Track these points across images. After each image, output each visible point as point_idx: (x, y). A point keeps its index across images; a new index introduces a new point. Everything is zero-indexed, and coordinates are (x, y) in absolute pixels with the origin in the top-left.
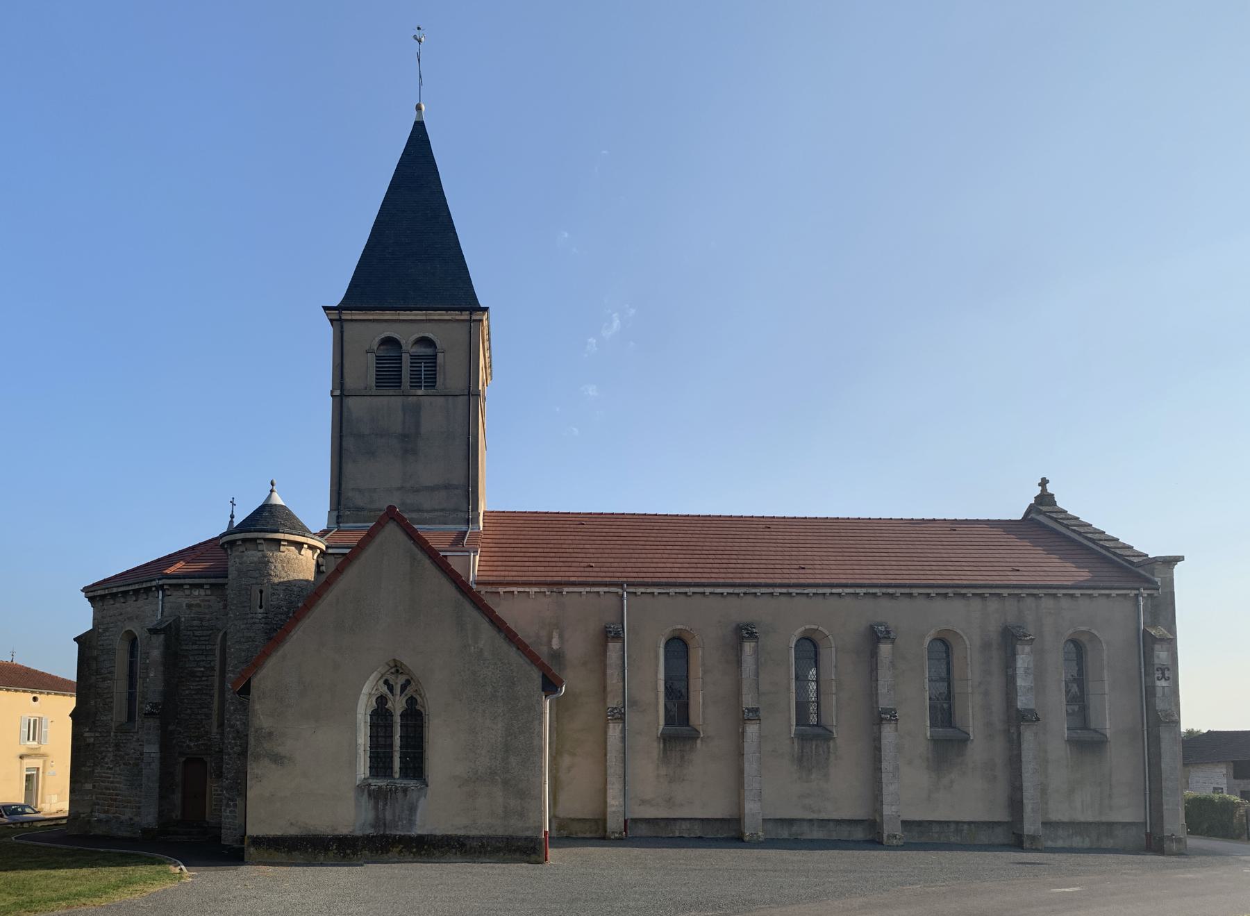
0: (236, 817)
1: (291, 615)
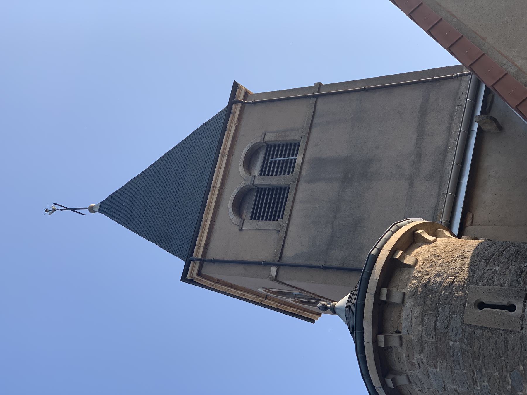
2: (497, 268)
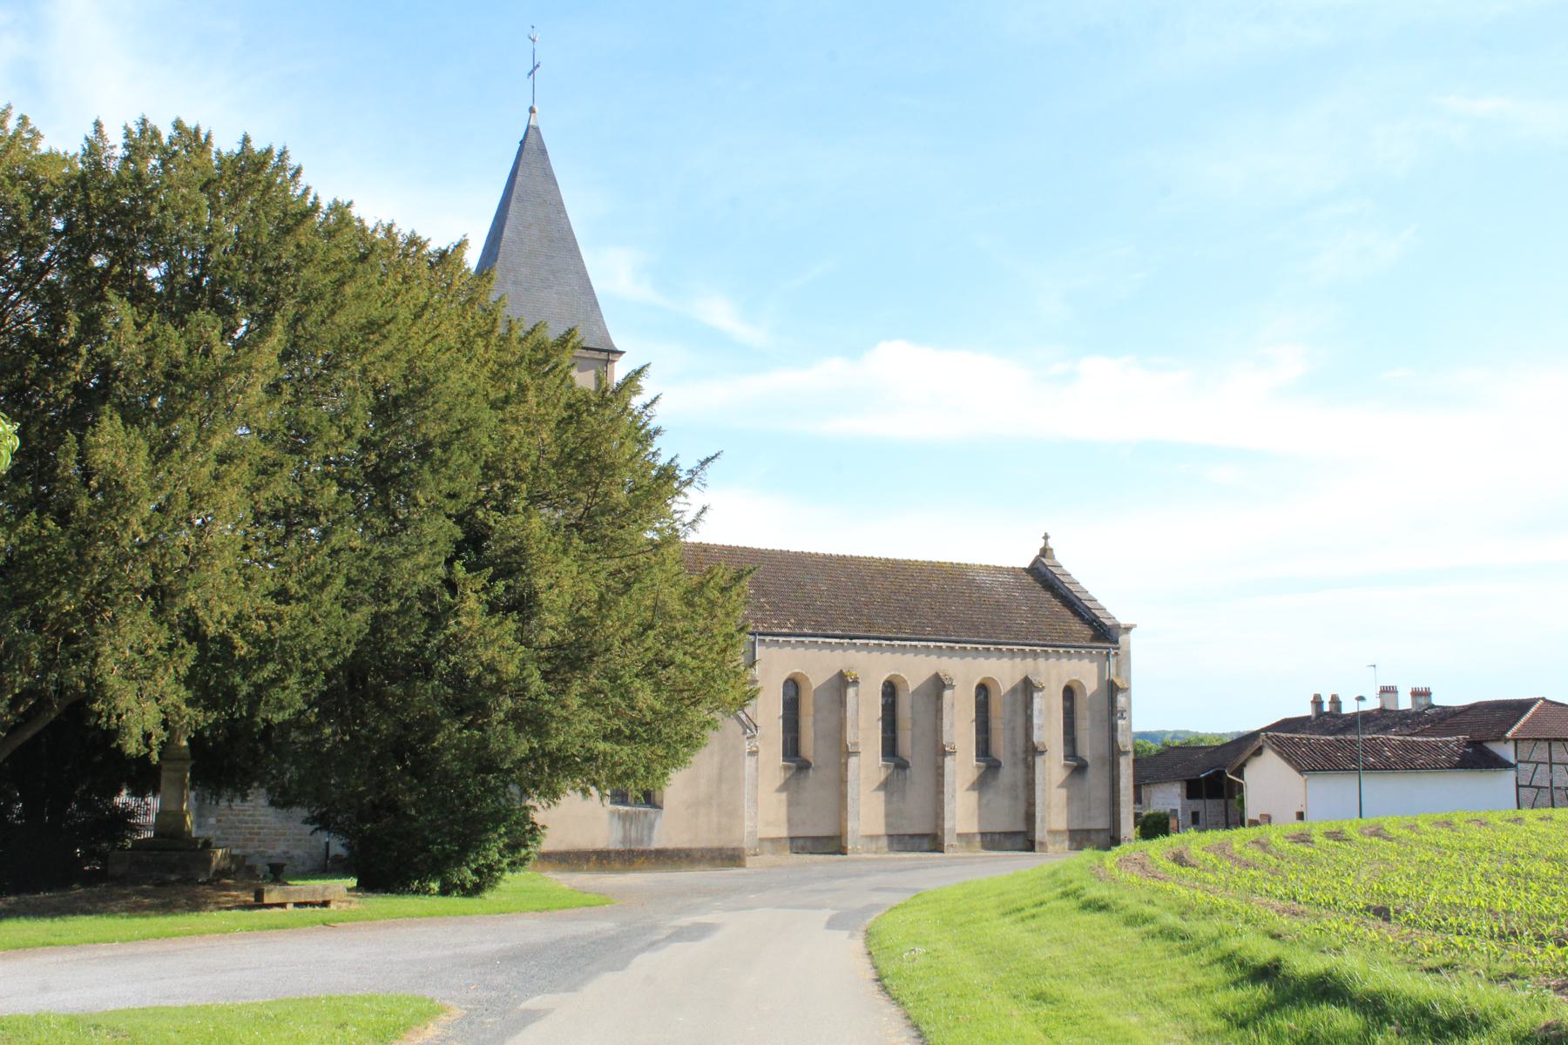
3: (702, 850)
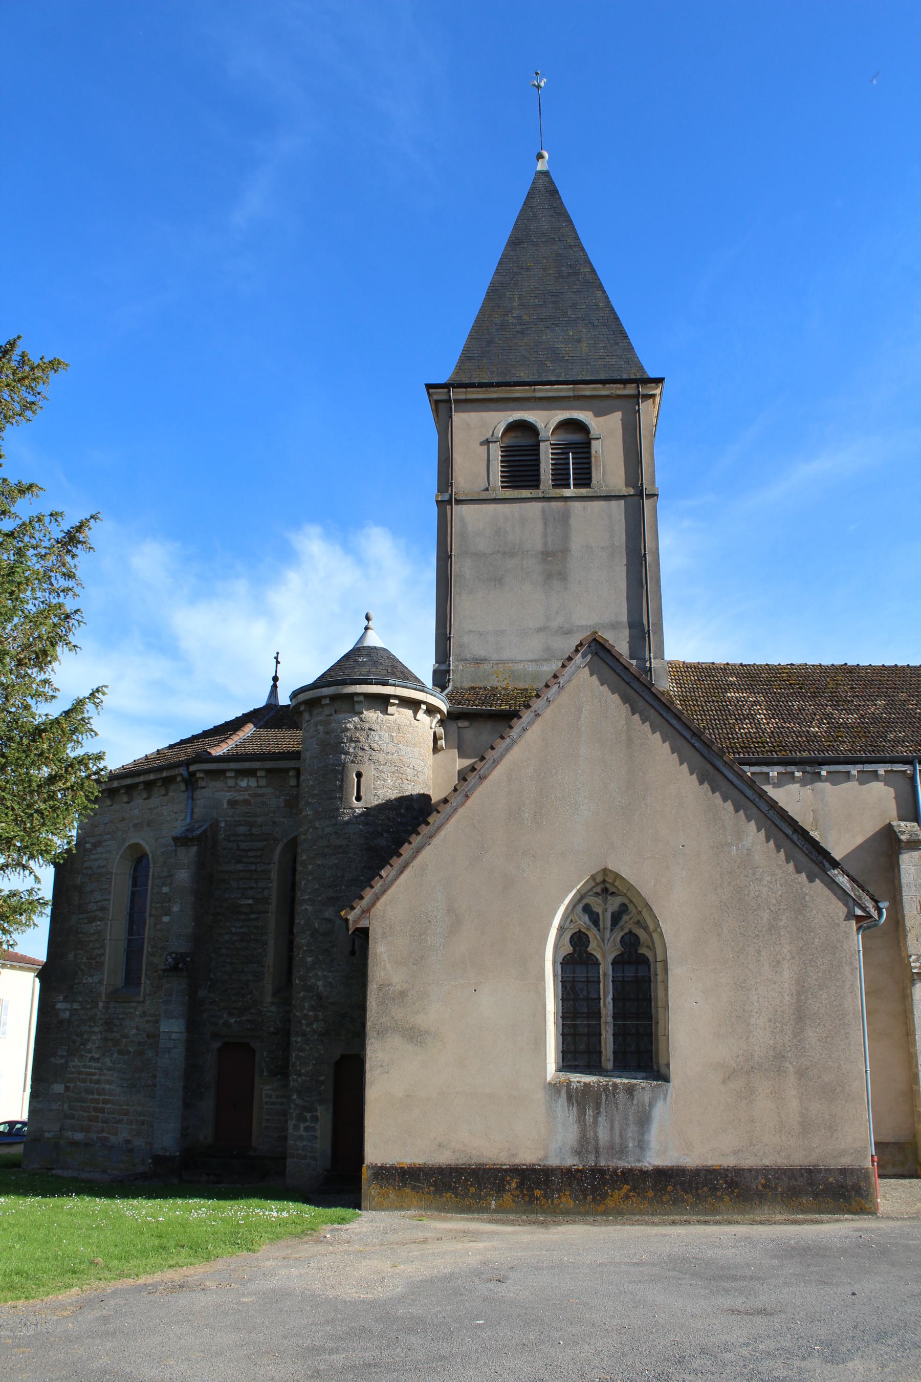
0: (316, 1138)
1: (403, 811)
2: (389, 781)
3: (765, 1171)
